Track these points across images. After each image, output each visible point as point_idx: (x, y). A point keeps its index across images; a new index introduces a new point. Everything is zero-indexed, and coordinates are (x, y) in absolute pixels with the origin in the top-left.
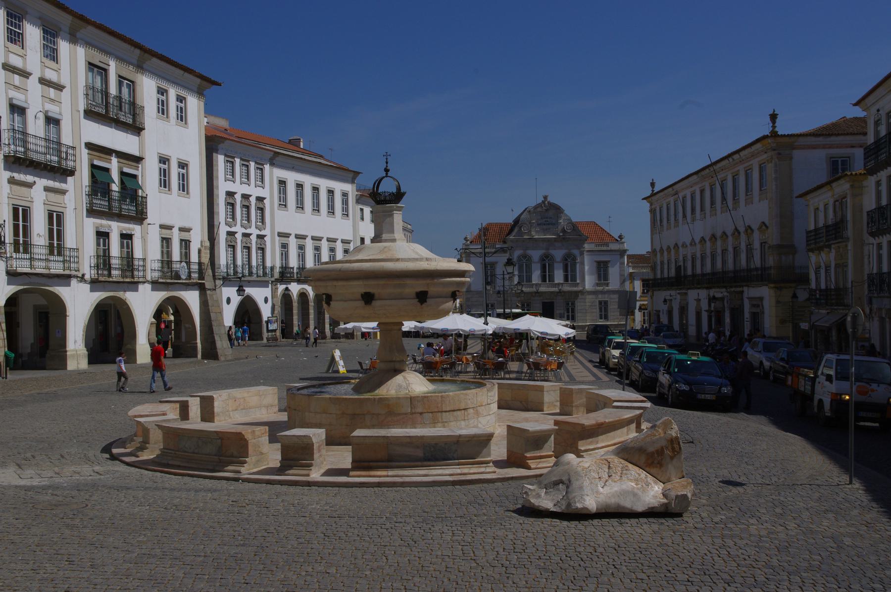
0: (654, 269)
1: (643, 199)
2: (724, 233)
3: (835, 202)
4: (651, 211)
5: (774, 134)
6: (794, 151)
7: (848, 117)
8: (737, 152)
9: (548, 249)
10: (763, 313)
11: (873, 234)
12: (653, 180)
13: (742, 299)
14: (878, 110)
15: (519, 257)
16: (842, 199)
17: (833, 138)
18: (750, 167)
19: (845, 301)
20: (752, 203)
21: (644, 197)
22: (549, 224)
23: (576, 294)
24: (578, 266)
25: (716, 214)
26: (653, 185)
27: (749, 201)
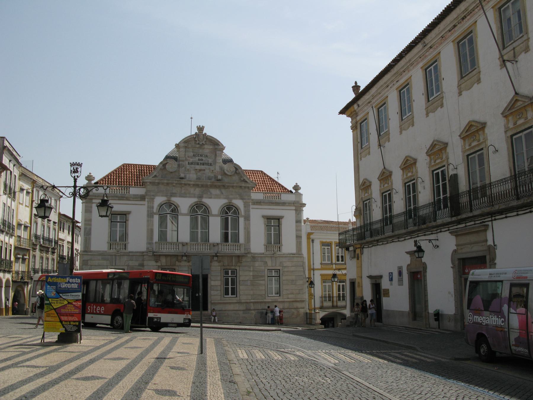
9: (201, 197)
12: (356, 83)
15: (161, 206)
22: (203, 164)
23: (239, 257)
24: (241, 220)
26: (356, 88)
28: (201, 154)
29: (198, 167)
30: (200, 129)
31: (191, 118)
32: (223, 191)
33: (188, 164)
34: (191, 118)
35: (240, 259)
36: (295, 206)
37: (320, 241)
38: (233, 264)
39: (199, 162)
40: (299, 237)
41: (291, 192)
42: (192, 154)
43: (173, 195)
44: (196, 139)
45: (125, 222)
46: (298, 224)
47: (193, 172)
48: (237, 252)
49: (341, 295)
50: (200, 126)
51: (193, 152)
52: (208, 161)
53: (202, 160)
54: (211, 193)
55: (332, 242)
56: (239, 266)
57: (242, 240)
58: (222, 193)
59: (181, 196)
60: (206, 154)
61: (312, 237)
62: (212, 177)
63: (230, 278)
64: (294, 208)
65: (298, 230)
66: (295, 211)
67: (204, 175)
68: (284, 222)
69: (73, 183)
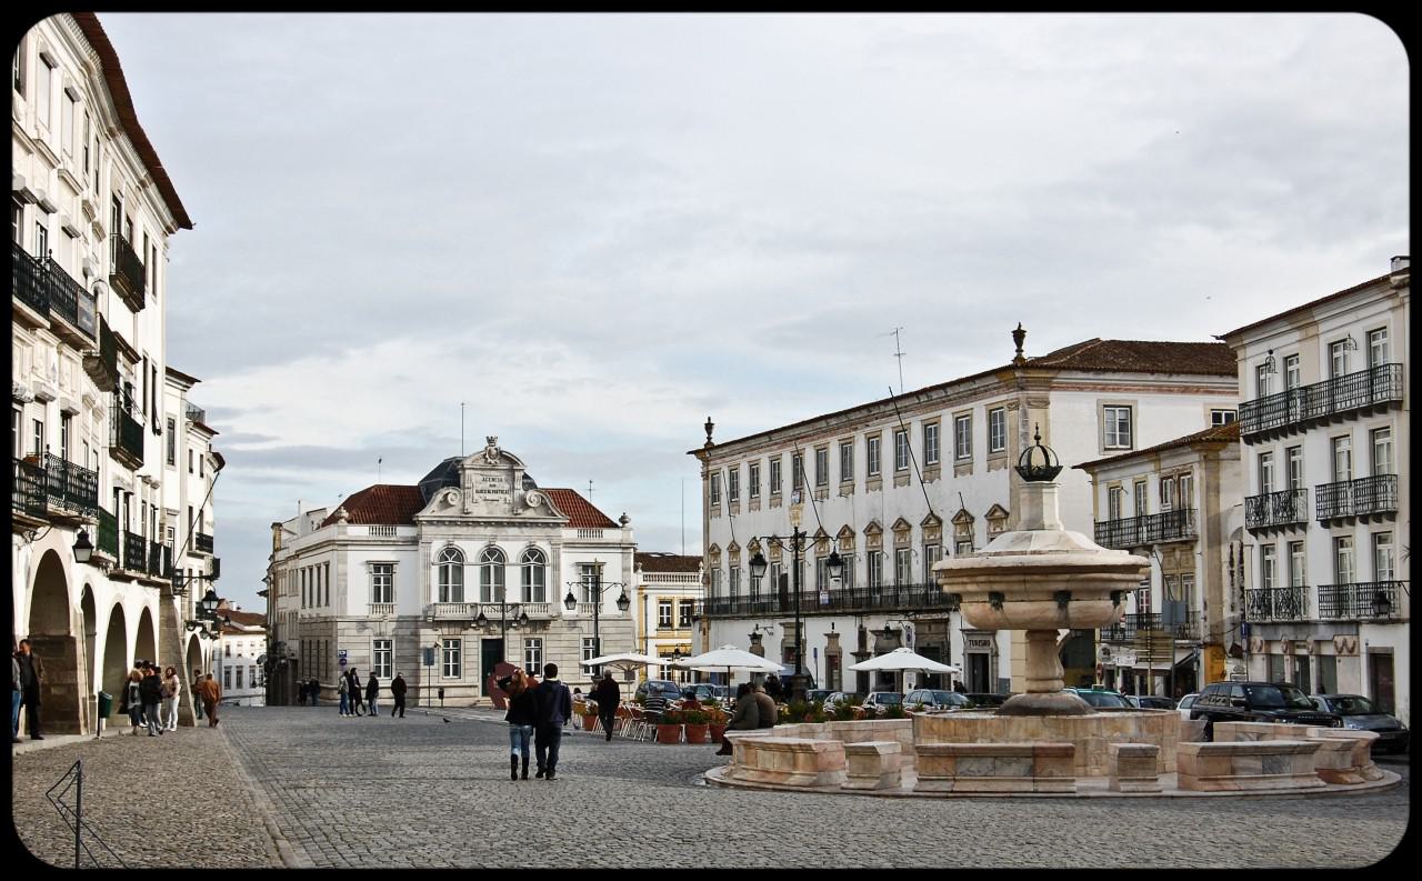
0: (709, 581)
1: (689, 453)
2: (901, 521)
3: (1162, 479)
4: (705, 476)
5: (1019, 358)
6: (1052, 393)
7: (1103, 339)
8: (943, 387)
10: (997, 655)
11: (1254, 532)
12: (709, 419)
13: (946, 633)
14: (1271, 352)
16: (1180, 476)
17: (1109, 376)
18: (969, 412)
19: (1192, 631)
20: (971, 473)
22: (496, 492)
23: (544, 624)
24: (548, 570)
25: (881, 488)
27: (963, 466)
29: (489, 496)
30: (491, 441)
41: (616, 526)
43: (457, 537)
47: (483, 503)
48: (543, 616)
57: (548, 599)
59: (467, 539)
63: (533, 652)
64: (620, 551)
66: (620, 555)
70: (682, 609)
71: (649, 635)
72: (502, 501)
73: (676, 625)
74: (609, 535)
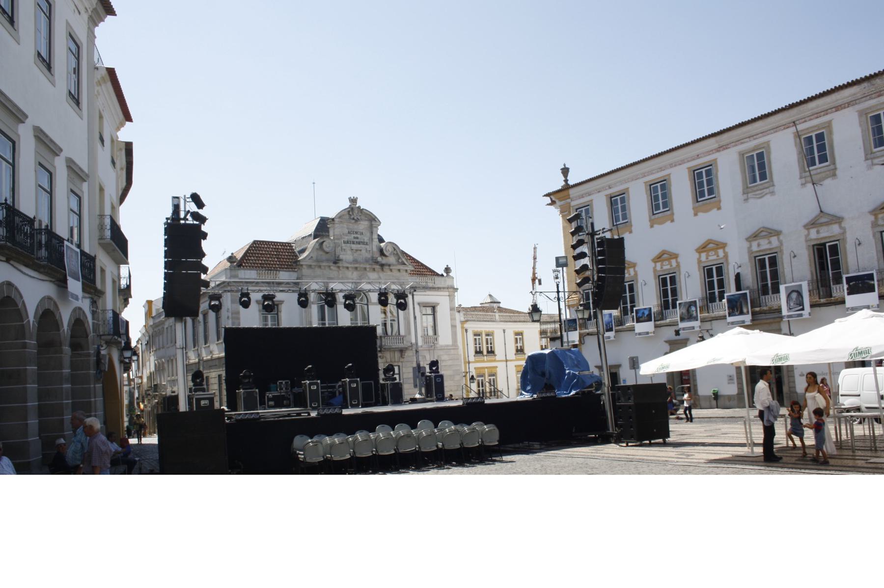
1: (545, 196)
12: (565, 165)
21: (547, 192)
22: (359, 243)
23: (402, 351)
26: (565, 171)
28: (355, 231)
29: (354, 246)
31: (314, 183)
32: (381, 274)
33: (344, 243)
34: (314, 183)
35: (403, 354)
36: (448, 291)
37: (473, 331)
38: (396, 360)
39: (355, 240)
40: (454, 327)
41: (442, 275)
42: (346, 231)
44: (351, 213)
45: (277, 314)
46: (452, 312)
47: (349, 252)
49: (481, 392)
50: (354, 197)
51: (348, 228)
52: (364, 239)
53: (357, 238)
54: (369, 278)
55: (482, 331)
56: (402, 362)
58: (380, 278)
60: (361, 231)
61: (466, 326)
62: (369, 258)
64: (447, 293)
65: (453, 319)
67: (361, 256)
68: (438, 309)
69: (556, 288)
70: (487, 339)
71: (470, 360)
72: (364, 251)
73: (485, 352)
74: (439, 282)
